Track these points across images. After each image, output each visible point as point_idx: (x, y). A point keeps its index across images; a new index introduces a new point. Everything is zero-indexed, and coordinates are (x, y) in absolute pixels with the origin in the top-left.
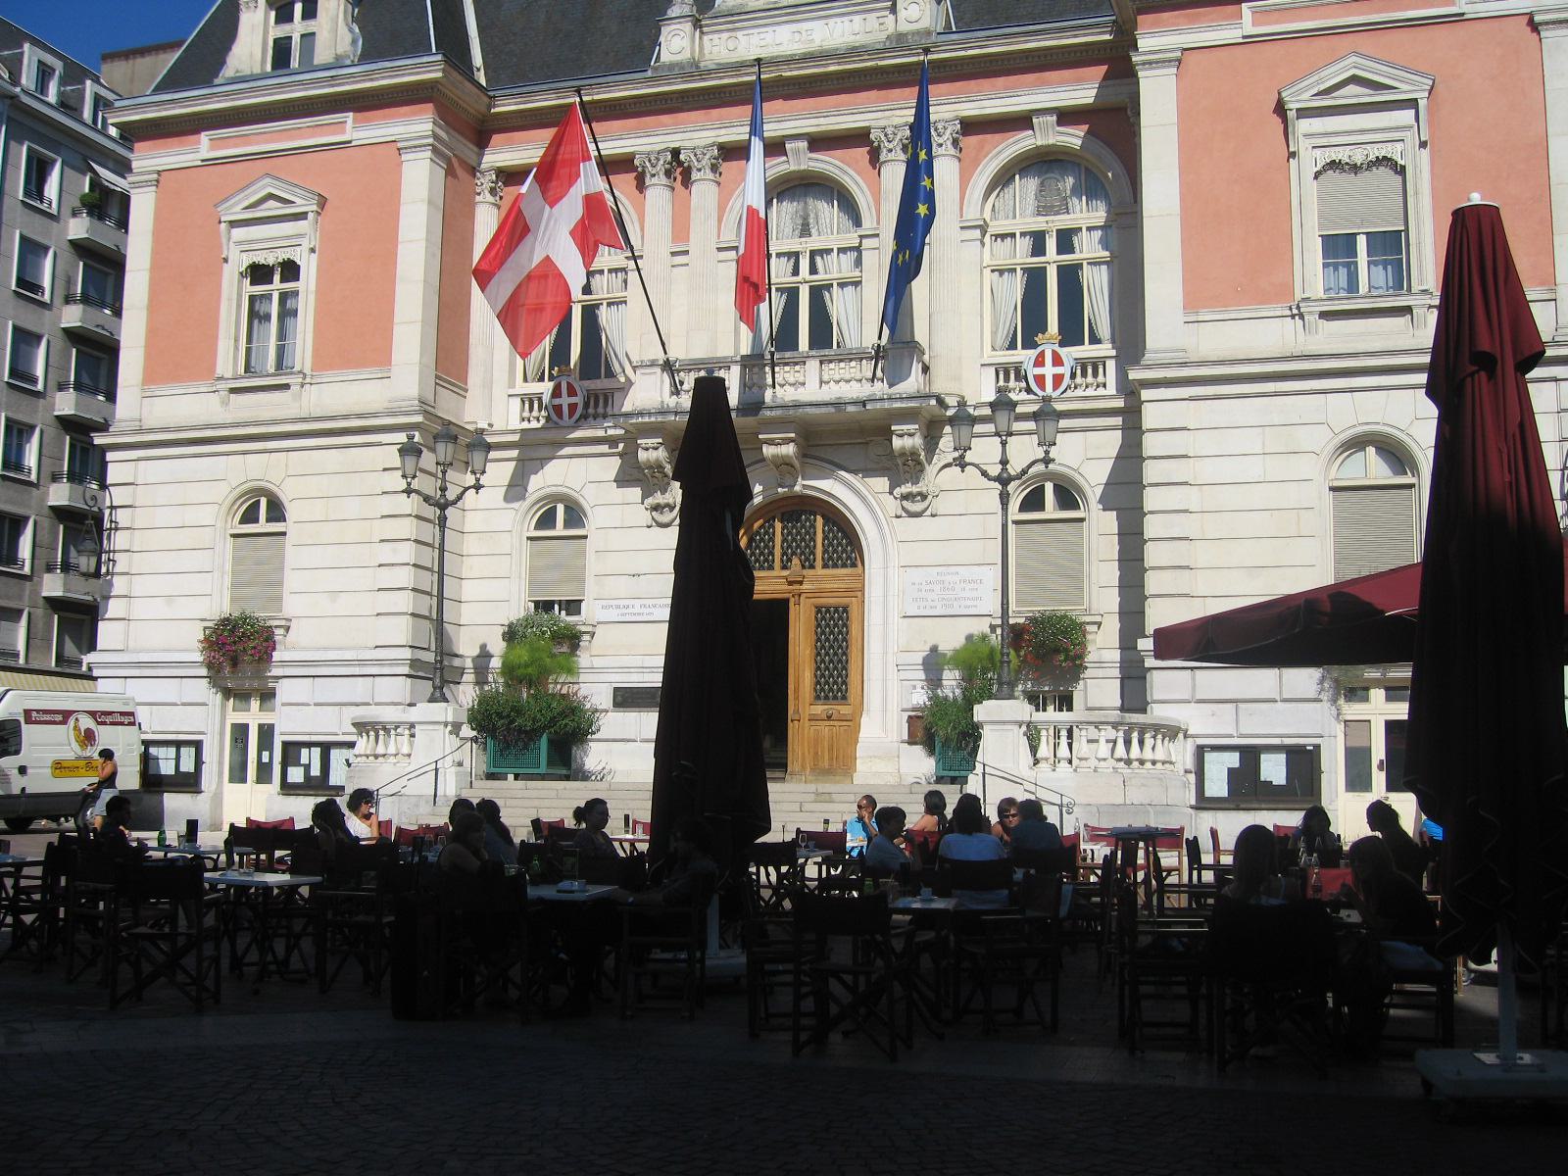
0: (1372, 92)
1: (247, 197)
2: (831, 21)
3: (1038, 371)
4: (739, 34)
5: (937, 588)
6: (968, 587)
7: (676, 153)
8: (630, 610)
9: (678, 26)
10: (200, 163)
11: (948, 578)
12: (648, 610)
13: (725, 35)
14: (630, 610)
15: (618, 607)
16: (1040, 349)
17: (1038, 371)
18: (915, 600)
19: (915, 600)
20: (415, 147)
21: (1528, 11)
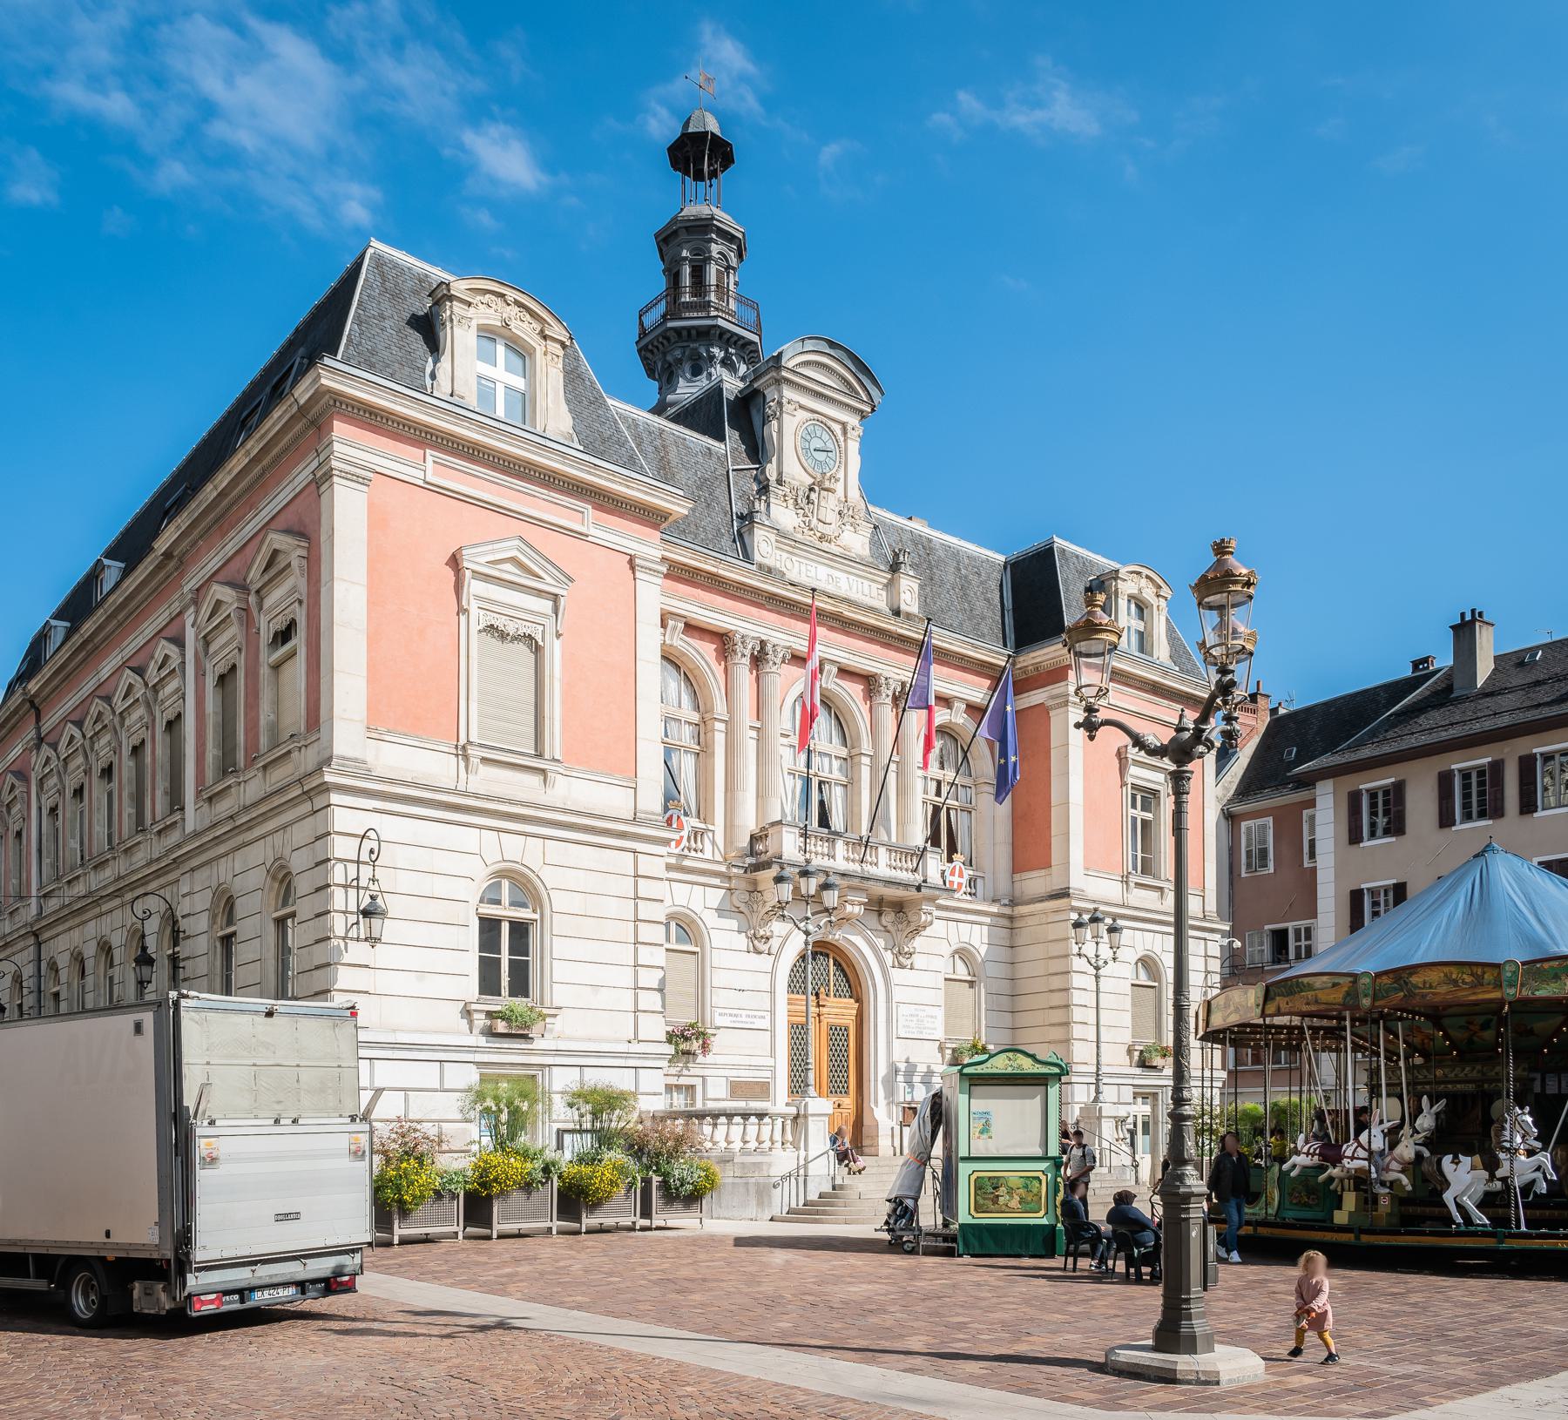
0: (519, 572)
1: (493, 552)
2: (852, 577)
3: (951, 878)
4: (794, 558)
5: (915, 1019)
6: (930, 1019)
7: (763, 643)
8: (739, 1019)
9: (766, 534)
10: (421, 483)
11: (921, 1013)
12: (752, 1020)
13: (785, 555)
14: (739, 1019)
15: (731, 1015)
16: (954, 864)
17: (951, 878)
18: (904, 1026)
19: (904, 1026)
20: (650, 570)
21: (633, 553)
